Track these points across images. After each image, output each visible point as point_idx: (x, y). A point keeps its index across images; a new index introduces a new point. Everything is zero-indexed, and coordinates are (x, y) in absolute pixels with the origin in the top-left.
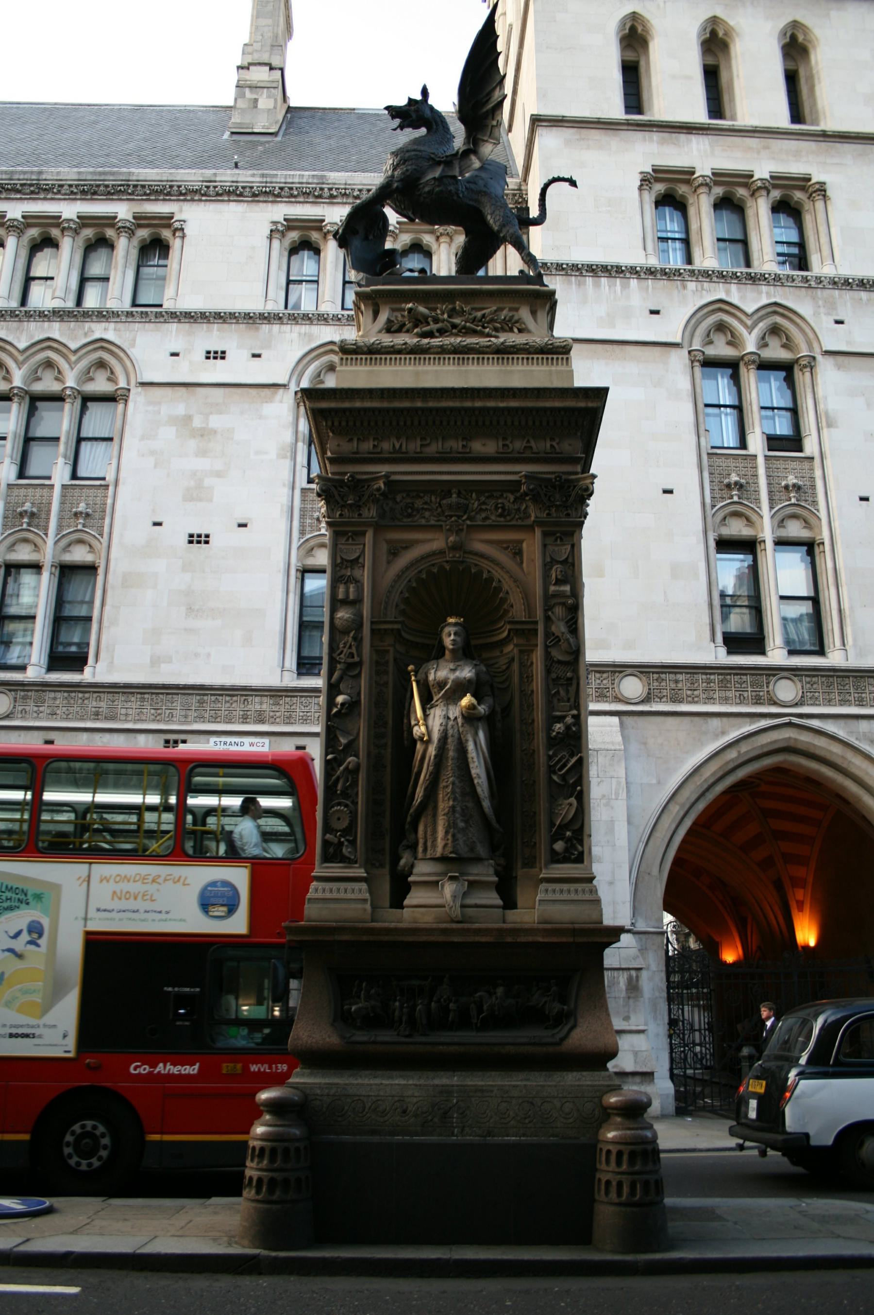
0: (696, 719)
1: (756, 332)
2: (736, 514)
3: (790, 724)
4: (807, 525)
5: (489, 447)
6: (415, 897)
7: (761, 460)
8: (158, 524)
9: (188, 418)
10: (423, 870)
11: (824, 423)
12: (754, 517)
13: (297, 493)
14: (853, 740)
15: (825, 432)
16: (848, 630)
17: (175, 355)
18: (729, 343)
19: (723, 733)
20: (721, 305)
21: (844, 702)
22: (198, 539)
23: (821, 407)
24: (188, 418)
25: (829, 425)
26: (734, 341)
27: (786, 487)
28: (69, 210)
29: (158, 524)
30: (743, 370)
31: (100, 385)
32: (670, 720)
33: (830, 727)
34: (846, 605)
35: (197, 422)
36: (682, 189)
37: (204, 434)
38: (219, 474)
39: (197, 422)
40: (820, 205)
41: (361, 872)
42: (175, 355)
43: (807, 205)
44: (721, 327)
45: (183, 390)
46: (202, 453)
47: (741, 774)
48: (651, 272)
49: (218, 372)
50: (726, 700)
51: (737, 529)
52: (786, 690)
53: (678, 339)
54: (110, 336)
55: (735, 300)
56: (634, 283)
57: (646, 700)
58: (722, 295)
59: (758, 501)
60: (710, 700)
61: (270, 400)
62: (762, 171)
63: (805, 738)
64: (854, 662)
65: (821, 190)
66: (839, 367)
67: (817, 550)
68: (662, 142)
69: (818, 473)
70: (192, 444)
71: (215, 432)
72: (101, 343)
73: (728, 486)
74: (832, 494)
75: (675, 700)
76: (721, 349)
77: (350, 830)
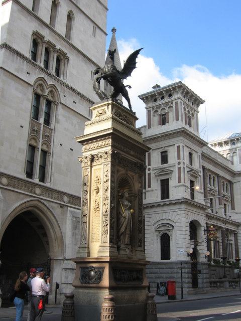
0: (18, 194)
1: (48, 90)
2: (33, 138)
3: (37, 200)
4: (48, 147)
5: (132, 153)
6: (122, 252)
7: (42, 126)
10: (122, 246)
11: (57, 121)
12: (38, 141)
14: (49, 207)
15: (57, 124)
16: (52, 178)
18: (41, 90)
19: (23, 199)
20: (43, 79)
21: (49, 197)
23: (57, 117)
25: (58, 123)
26: (42, 90)
27: (46, 135)
30: (42, 98)
32: (12, 193)
33: (45, 203)
34: (53, 171)
36: (39, 40)
40: (66, 62)
43: (63, 61)
44: (41, 85)
47: (23, 211)
48: (30, 61)
50: (25, 190)
51: (33, 143)
52: (38, 191)
53: (32, 84)
55: (46, 79)
56: (25, 62)
57: (7, 186)
58: (43, 77)
59: (39, 136)
60: (21, 189)
62: (58, 47)
63: (40, 204)
64: (52, 187)
65: (68, 59)
66: (63, 108)
67: (47, 154)
68: (39, 25)
69: (53, 134)
73: (34, 130)
74: (55, 141)
75: (14, 187)
76: (39, 91)
77: (113, 236)
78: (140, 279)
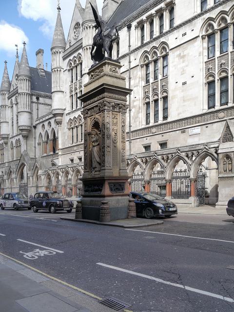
8: (177, 83)
9: (180, 54)
13: (204, 63)
17: (176, 39)
22: (184, 83)
24: (180, 54)
28: (153, 11)
29: (177, 83)
31: (164, 53)
35: (182, 54)
37: (184, 56)
38: (187, 66)
39: (182, 54)
41: (87, 171)
42: (176, 39)
45: (178, 47)
46: (183, 62)
49: (187, 38)
54: (164, 40)
61: (196, 41)
70: (181, 60)
71: (185, 55)
72: (164, 43)
78: (101, 190)
